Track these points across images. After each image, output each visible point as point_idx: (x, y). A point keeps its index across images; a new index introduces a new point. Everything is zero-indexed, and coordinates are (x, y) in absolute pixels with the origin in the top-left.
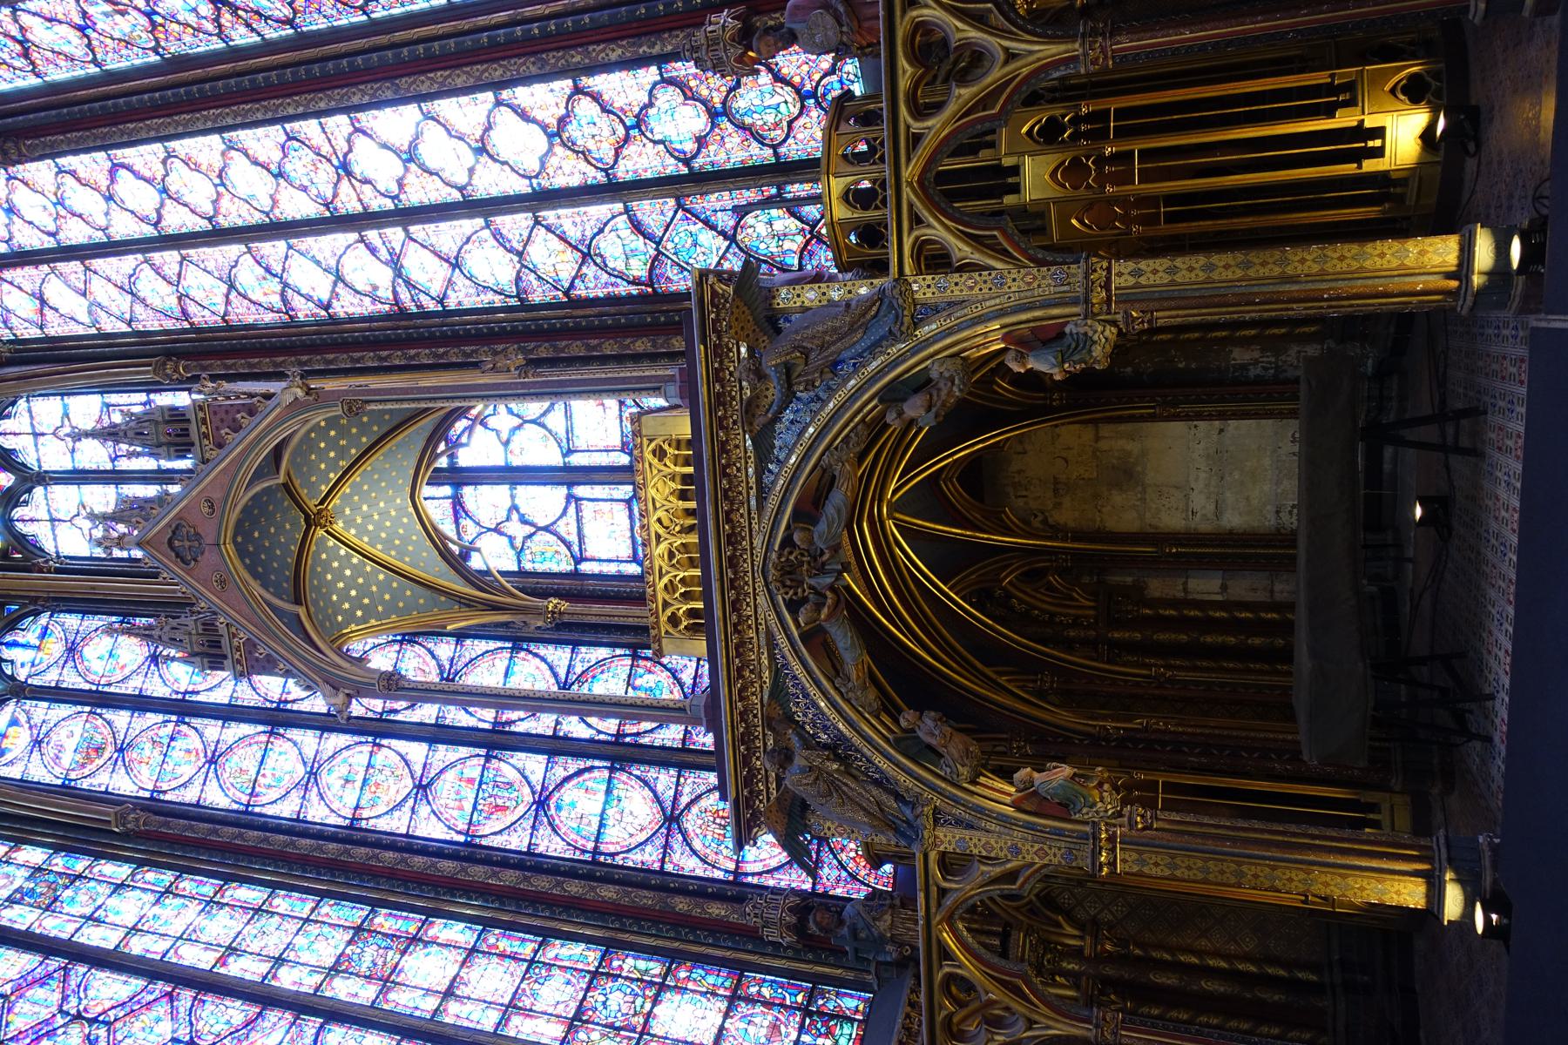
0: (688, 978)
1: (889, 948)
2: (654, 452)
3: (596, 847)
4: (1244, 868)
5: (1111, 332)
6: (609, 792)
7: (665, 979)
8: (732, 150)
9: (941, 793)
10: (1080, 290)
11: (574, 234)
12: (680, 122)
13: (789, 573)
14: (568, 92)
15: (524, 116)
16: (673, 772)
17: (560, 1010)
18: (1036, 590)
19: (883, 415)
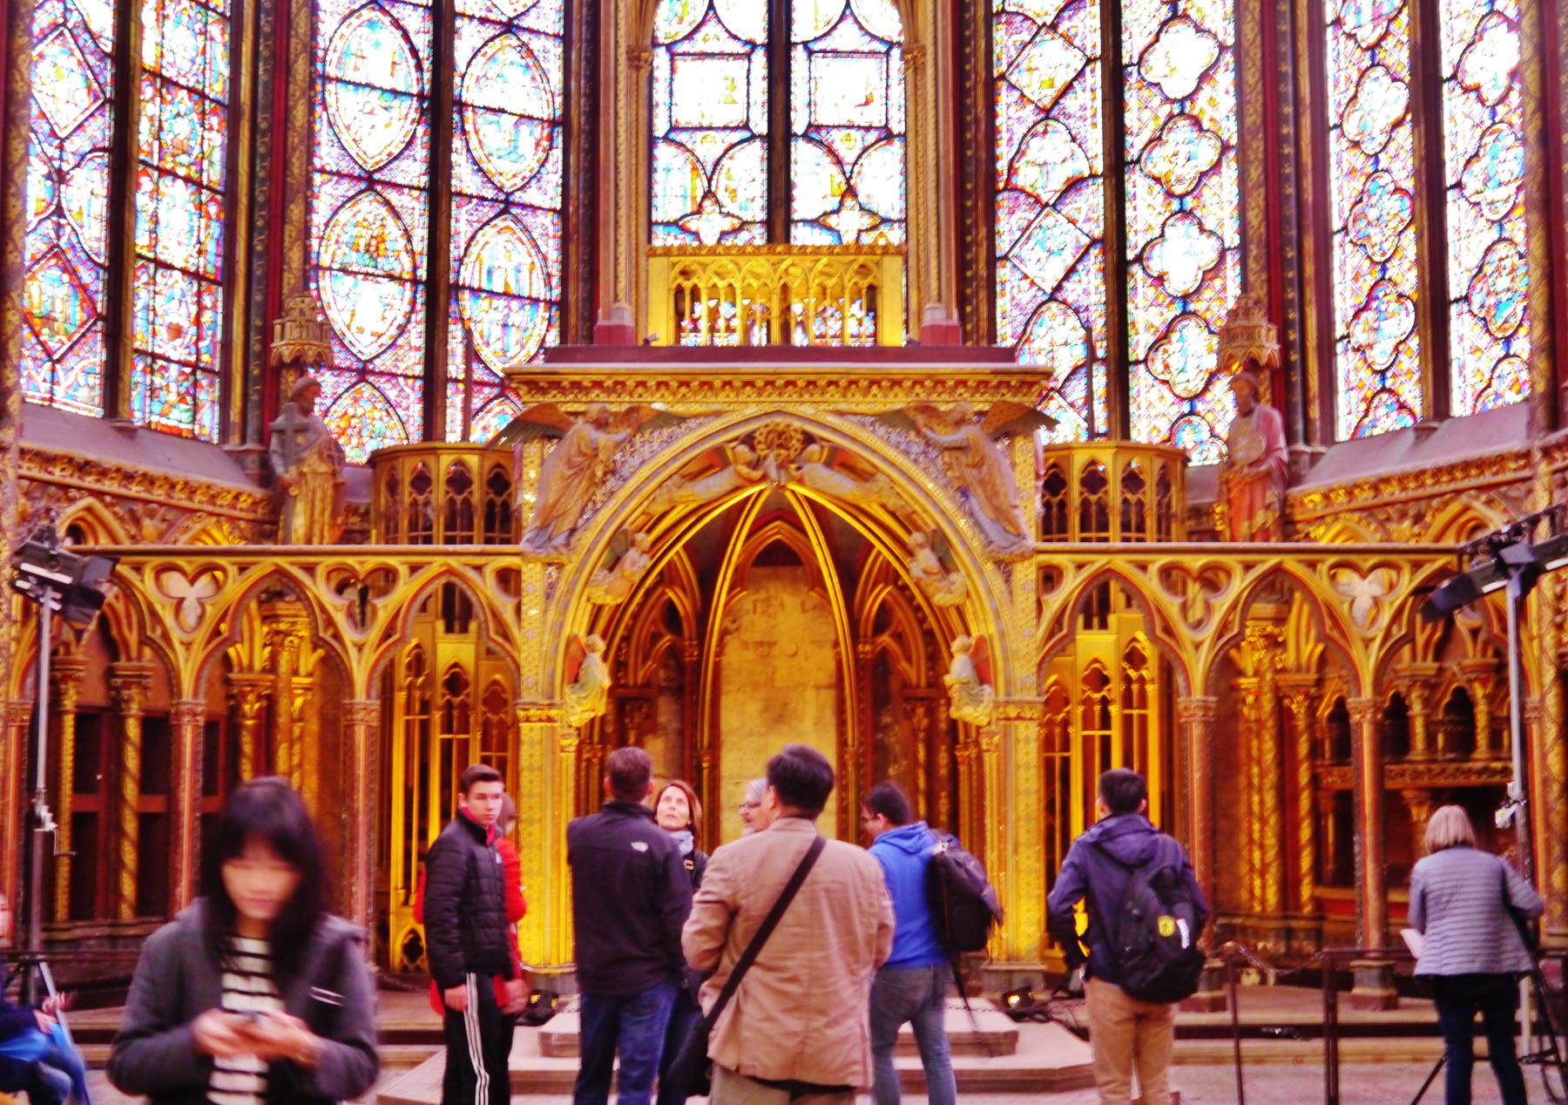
0: (209, 218)
1: (293, 471)
2: (862, 266)
3: (330, 80)
4: (536, 826)
5: (983, 721)
6: (395, 93)
7: (208, 188)
8: (1145, 315)
9: (579, 571)
10: (1016, 697)
11: (1070, 103)
12: (1181, 256)
13: (780, 439)
14: (1225, 137)
15: (1205, 77)
16: (425, 179)
17: (168, 57)
18: (653, 622)
19: (918, 529)
